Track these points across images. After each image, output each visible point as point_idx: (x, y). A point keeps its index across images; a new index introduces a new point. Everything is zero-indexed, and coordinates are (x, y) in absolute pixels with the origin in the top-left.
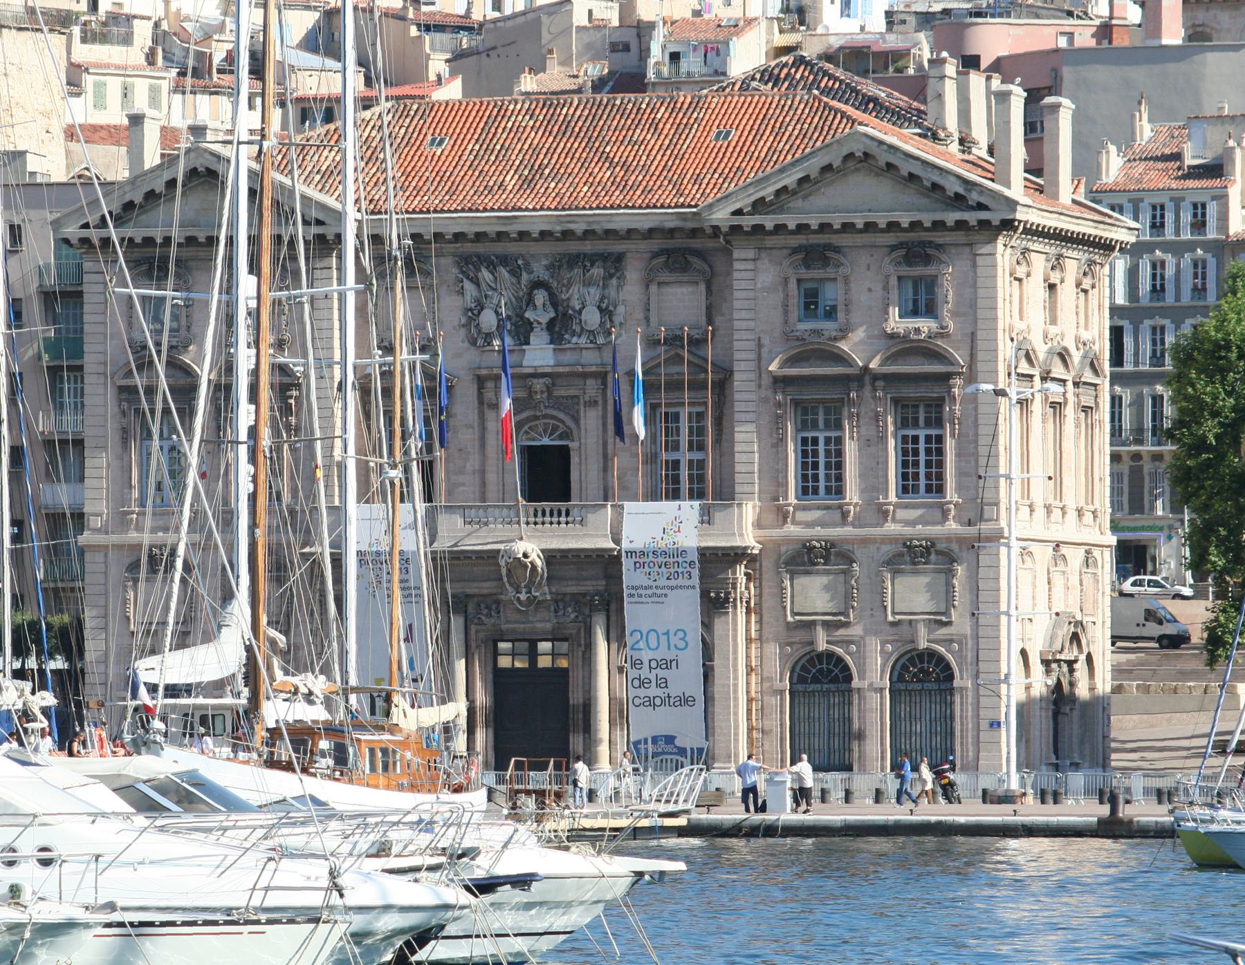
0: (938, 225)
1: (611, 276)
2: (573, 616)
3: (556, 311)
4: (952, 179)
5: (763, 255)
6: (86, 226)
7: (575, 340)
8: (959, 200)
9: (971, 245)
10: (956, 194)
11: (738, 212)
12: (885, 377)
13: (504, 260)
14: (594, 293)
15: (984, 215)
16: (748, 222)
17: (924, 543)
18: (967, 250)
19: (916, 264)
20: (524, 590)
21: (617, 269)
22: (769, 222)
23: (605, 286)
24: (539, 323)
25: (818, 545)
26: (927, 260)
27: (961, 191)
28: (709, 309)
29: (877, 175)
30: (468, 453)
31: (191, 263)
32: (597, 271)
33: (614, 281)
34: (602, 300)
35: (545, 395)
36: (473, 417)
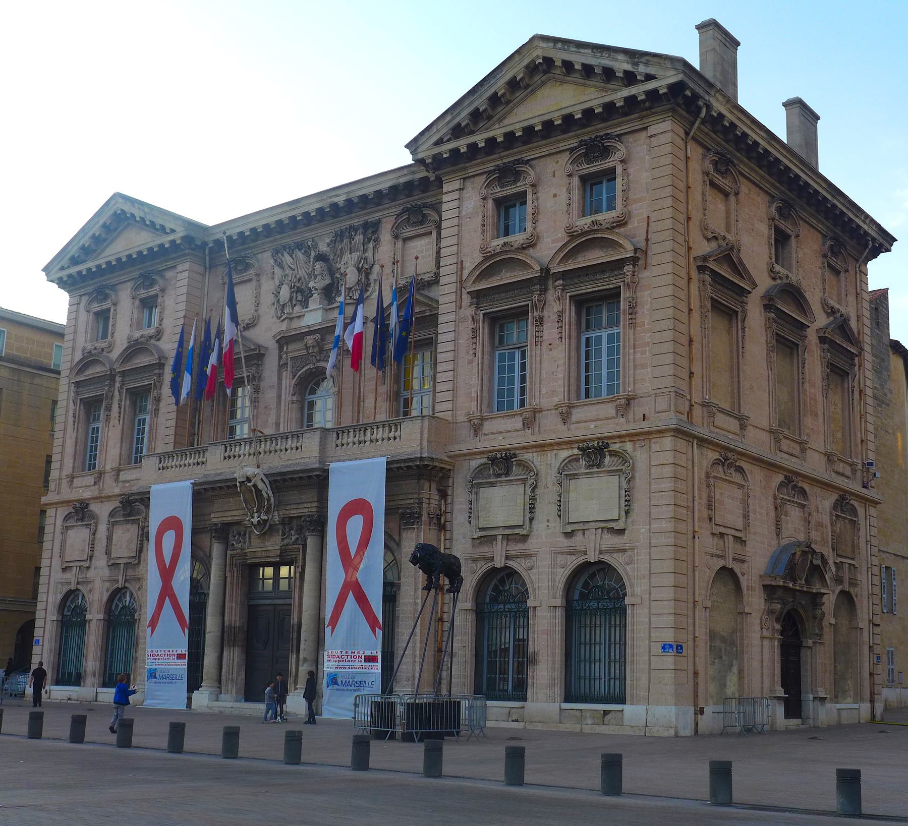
2: (294, 538)
3: (332, 279)
4: (621, 57)
5: (468, 183)
6: (62, 268)
8: (630, 78)
11: (439, 142)
12: (564, 275)
13: (299, 246)
15: (651, 85)
18: (643, 134)
19: (596, 159)
20: (256, 515)
21: (374, 233)
23: (365, 251)
24: (316, 289)
25: (499, 456)
26: (606, 152)
27: (628, 67)
30: (271, 409)
31: (119, 287)
32: (359, 238)
33: (371, 245)
35: (316, 349)
36: (275, 379)
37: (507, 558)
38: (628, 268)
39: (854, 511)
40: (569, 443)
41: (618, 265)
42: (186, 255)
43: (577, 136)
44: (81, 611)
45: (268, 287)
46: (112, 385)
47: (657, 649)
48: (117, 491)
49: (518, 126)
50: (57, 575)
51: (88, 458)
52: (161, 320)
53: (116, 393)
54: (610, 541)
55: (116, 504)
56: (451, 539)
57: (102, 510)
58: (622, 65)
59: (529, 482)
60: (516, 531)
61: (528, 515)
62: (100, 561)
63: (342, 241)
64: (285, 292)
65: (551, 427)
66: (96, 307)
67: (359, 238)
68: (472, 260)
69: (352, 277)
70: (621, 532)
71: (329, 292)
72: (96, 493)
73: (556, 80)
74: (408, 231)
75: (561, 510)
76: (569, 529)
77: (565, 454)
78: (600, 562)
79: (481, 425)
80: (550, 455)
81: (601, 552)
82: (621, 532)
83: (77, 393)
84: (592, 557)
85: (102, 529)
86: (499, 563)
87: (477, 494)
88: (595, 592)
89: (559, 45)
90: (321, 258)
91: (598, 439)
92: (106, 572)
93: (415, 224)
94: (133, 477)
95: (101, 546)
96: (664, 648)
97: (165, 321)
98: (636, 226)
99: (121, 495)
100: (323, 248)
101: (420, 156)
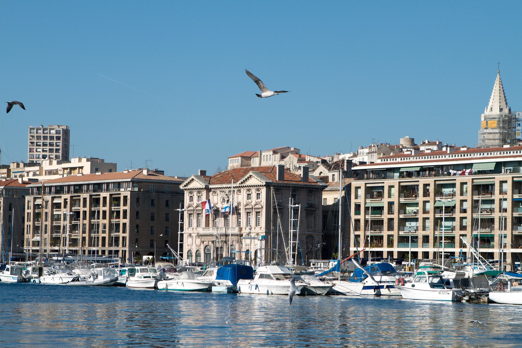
16: (240, 185)
22: (242, 185)
39: (313, 237)
44: (191, 253)
45: (219, 197)
50: (187, 247)
51: (190, 225)
55: (196, 234)
57: (194, 235)
62: (194, 245)
64: (222, 200)
66: (190, 195)
68: (245, 203)
71: (228, 201)
85: (194, 239)
90: (227, 195)
92: (195, 247)
95: (194, 242)
98: (262, 203)
100: (227, 193)
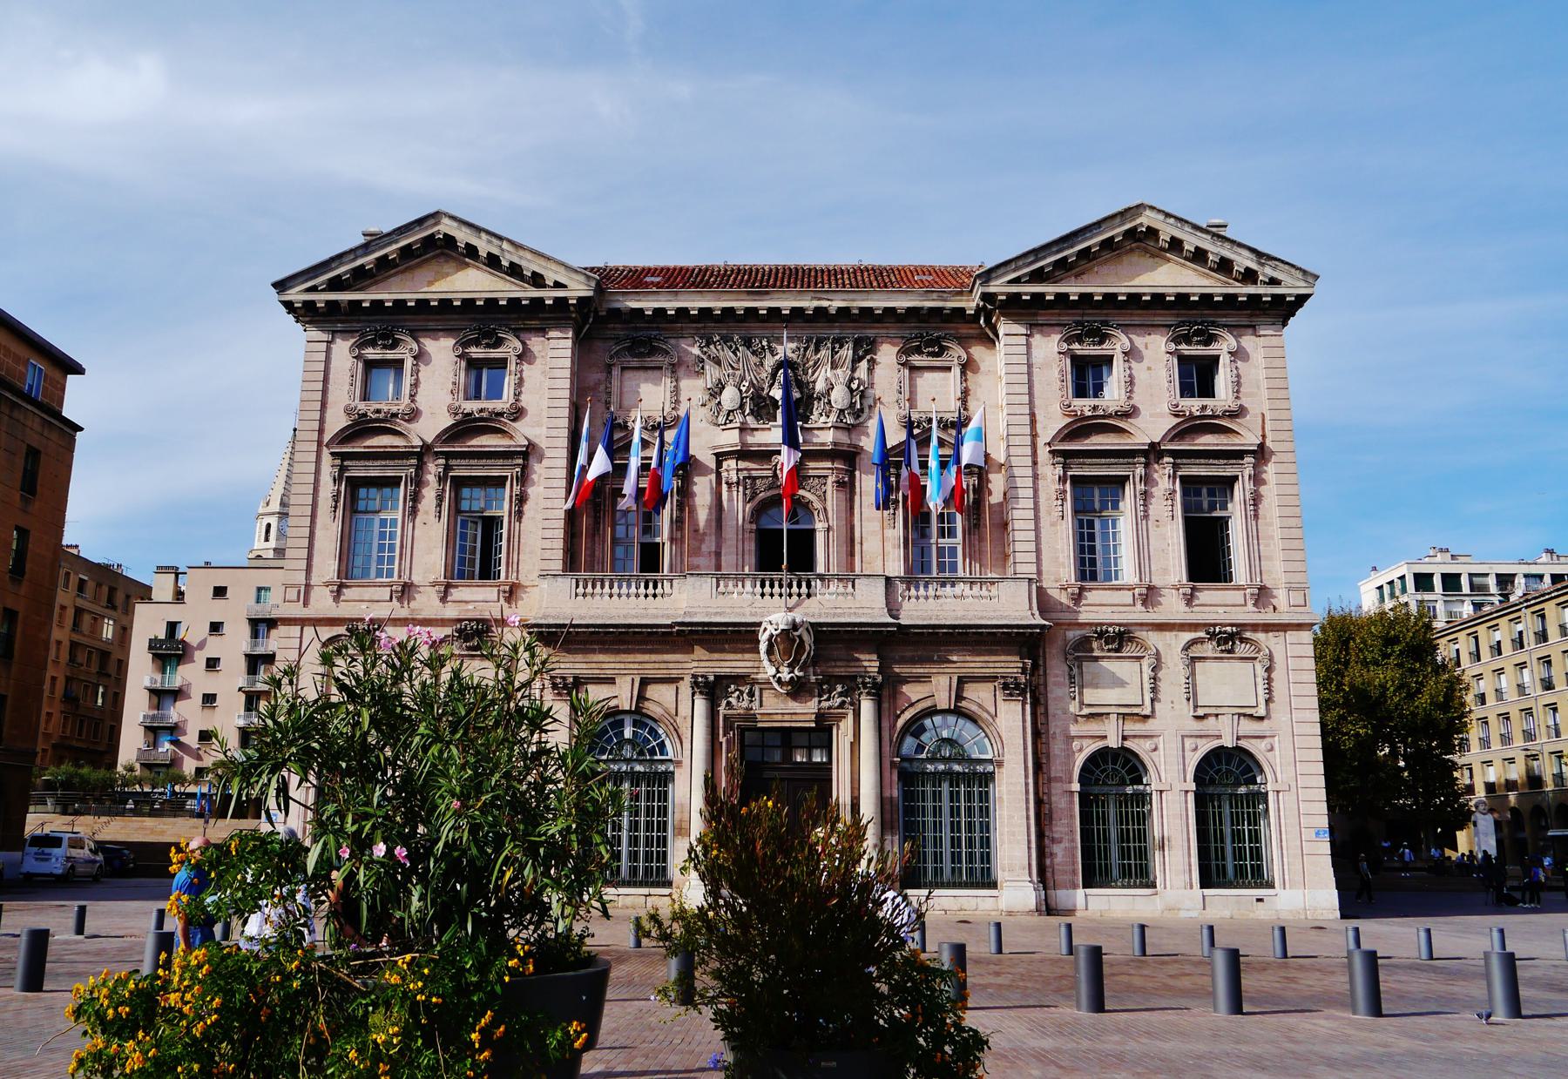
0: (1230, 299)
1: (861, 359)
4: (1246, 253)
6: (313, 289)
7: (823, 419)
8: (1249, 276)
9: (1254, 327)
10: (1247, 269)
14: (842, 374)
17: (1229, 629)
18: (1250, 331)
19: (1199, 343)
20: (786, 670)
21: (867, 352)
23: (854, 370)
27: (1254, 266)
28: (965, 393)
29: (1153, 256)
33: (864, 364)
34: (851, 380)
37: (1124, 738)
38: (1249, 459)
40: (1194, 627)
41: (1239, 455)
42: (570, 318)
43: (1178, 315)
46: (420, 468)
47: (1308, 834)
48: (451, 612)
49: (1124, 290)
52: (517, 395)
53: (431, 478)
54: (1247, 727)
56: (1046, 714)
58: (1243, 261)
59: (1145, 662)
60: (1136, 710)
61: (1148, 696)
63: (817, 351)
65: (1172, 607)
67: (847, 352)
69: (839, 397)
70: (1261, 718)
72: (403, 613)
73: (1146, 251)
74: (917, 360)
75: (1192, 695)
76: (1200, 712)
77: (1188, 636)
78: (1238, 749)
79: (1080, 595)
80: (1169, 636)
81: (1238, 738)
82: (1261, 718)
83: (342, 469)
84: (1228, 742)
86: (1113, 742)
87: (1080, 667)
88: (1228, 780)
89: (1172, 221)
91: (1232, 625)
93: (929, 354)
94: (480, 598)
96: (1317, 834)
97: (522, 397)
99: (460, 621)
101: (992, 290)
